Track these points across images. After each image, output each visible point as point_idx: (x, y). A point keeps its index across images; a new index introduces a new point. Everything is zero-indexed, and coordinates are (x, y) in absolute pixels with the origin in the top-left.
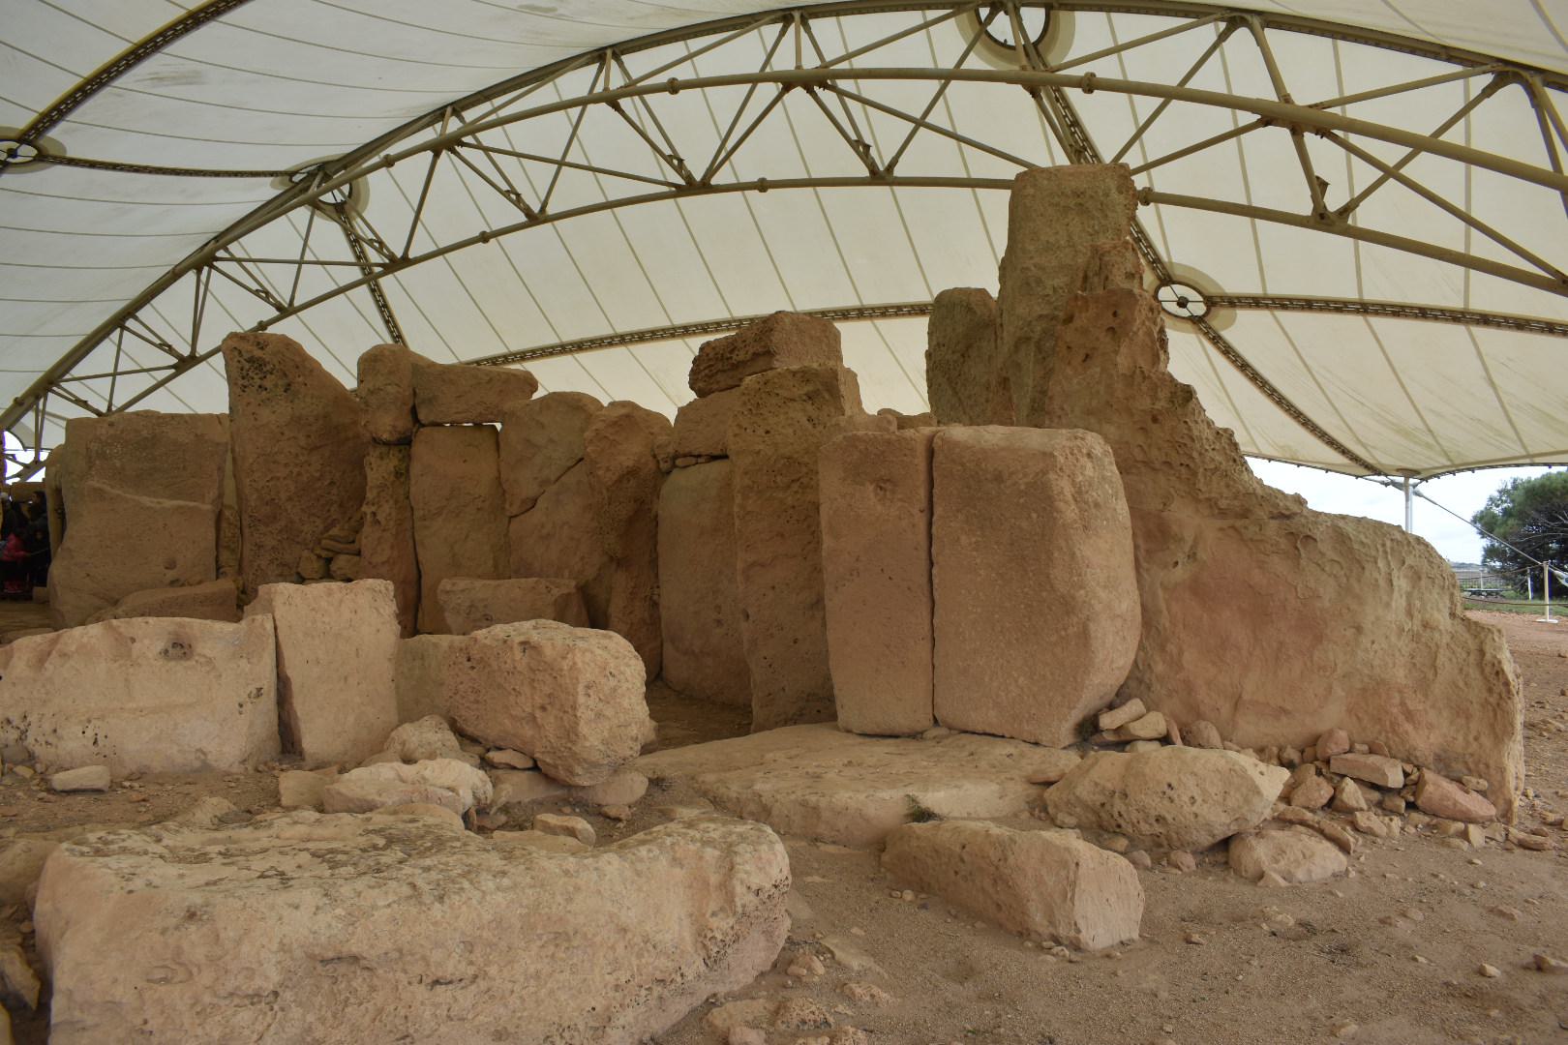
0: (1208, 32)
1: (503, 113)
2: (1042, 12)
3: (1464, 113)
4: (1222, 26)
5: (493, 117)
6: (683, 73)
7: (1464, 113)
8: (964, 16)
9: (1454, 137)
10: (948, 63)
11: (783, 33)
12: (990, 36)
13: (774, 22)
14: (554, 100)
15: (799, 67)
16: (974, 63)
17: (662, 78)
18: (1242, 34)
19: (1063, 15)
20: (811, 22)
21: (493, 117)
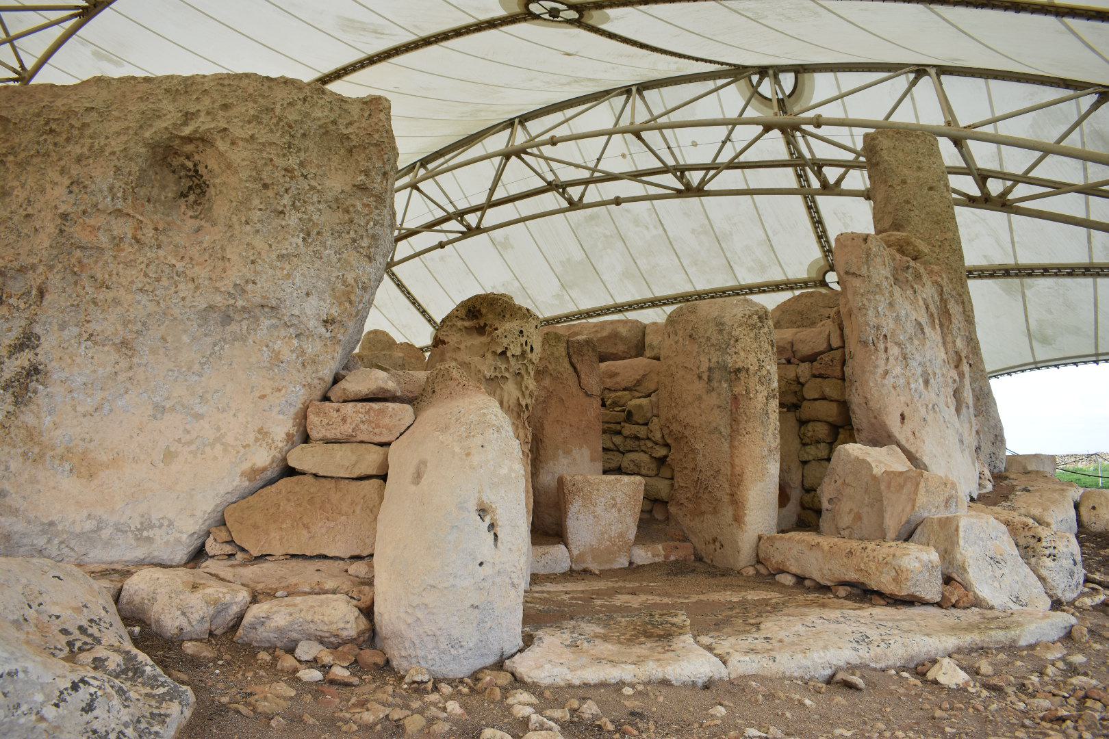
0: (902, 81)
1: (451, 163)
2: (792, 75)
3: (1078, 124)
4: (912, 76)
5: (445, 166)
6: (558, 133)
7: (1078, 124)
8: (742, 81)
9: (1074, 141)
10: (733, 114)
11: (627, 101)
12: (761, 95)
13: (621, 94)
14: (483, 153)
15: (632, 123)
16: (751, 113)
17: (547, 137)
18: (926, 83)
19: (806, 76)
20: (645, 93)
21: (445, 166)
